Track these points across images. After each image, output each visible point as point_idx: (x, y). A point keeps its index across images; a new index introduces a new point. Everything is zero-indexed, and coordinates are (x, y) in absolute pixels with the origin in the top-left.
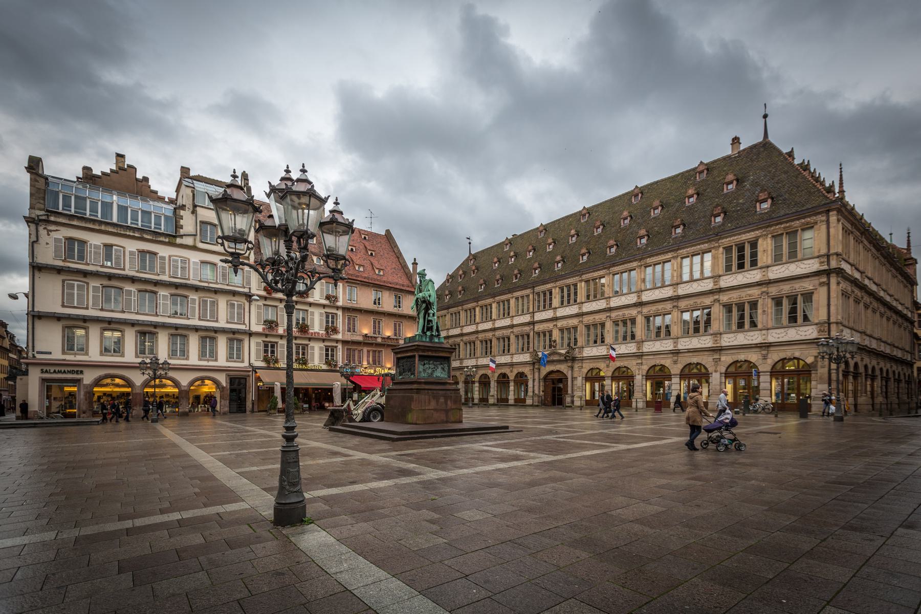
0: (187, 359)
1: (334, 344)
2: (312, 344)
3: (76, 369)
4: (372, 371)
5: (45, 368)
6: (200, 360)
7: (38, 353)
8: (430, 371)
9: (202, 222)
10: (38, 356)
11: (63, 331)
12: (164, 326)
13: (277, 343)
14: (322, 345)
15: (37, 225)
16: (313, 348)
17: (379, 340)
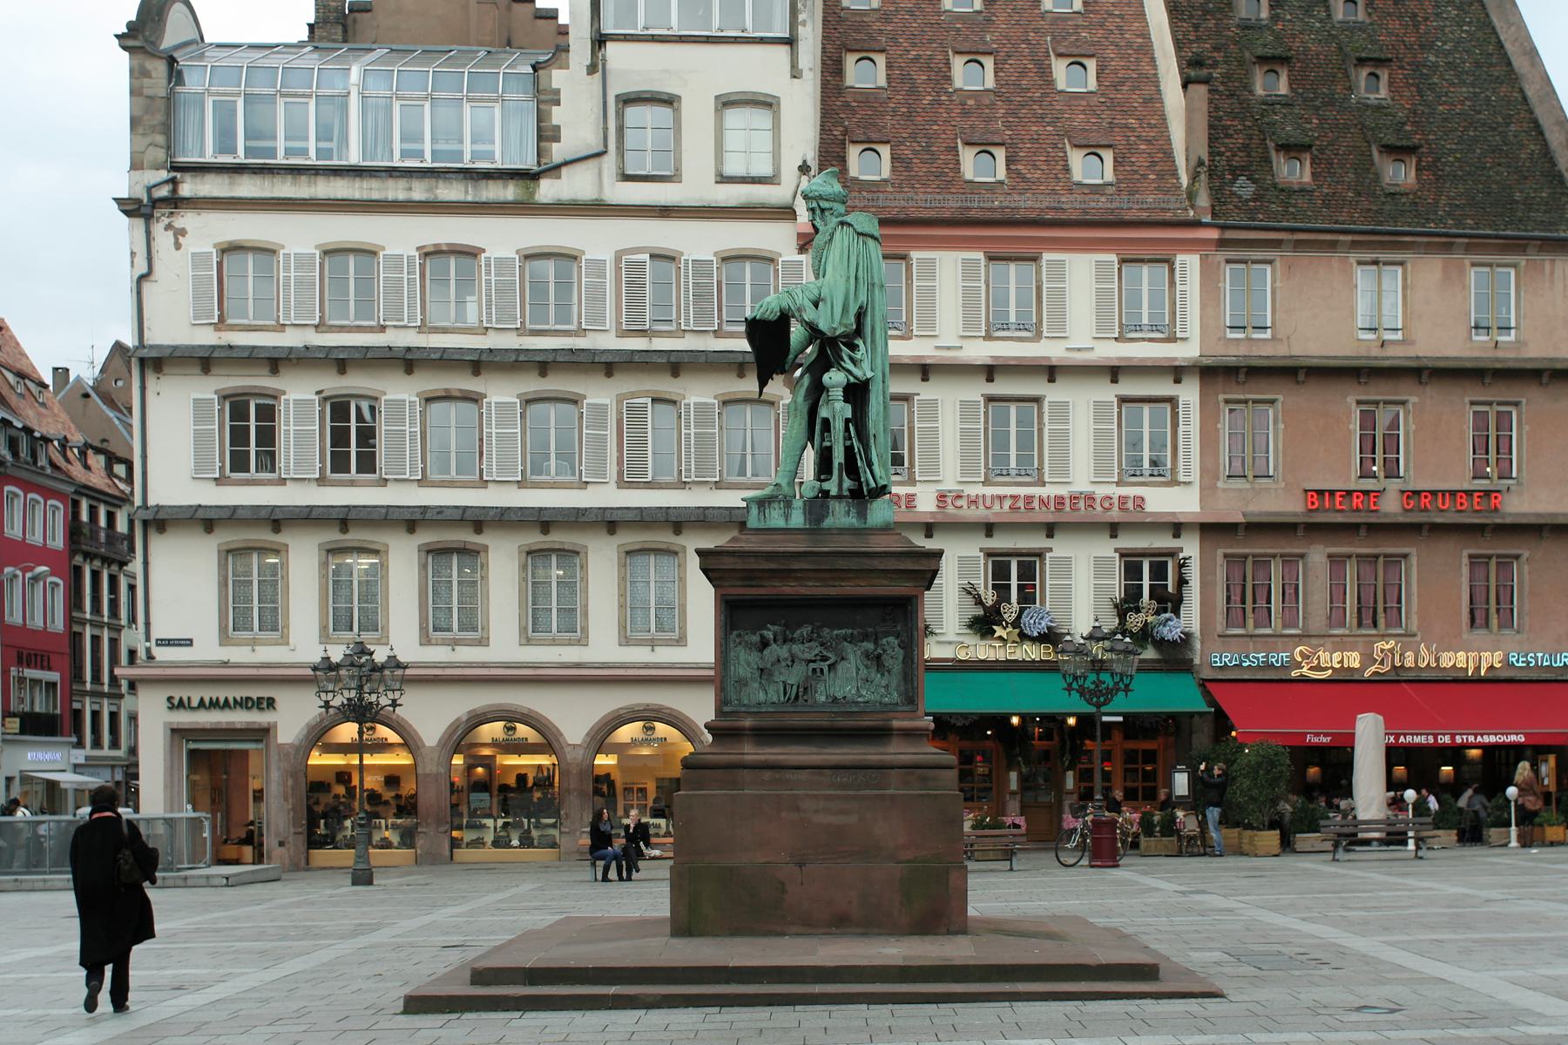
0: (583, 641)
1: (1164, 542)
2: (1060, 548)
3: (255, 692)
4: (1354, 660)
5: (178, 693)
6: (527, 641)
7: (162, 643)
8: (795, 676)
9: (627, 100)
10: (162, 654)
11: (223, 567)
12: (506, 520)
13: (1040, 554)
14: (1106, 548)
15: (148, 218)
16: (1065, 565)
17: (1391, 506)
